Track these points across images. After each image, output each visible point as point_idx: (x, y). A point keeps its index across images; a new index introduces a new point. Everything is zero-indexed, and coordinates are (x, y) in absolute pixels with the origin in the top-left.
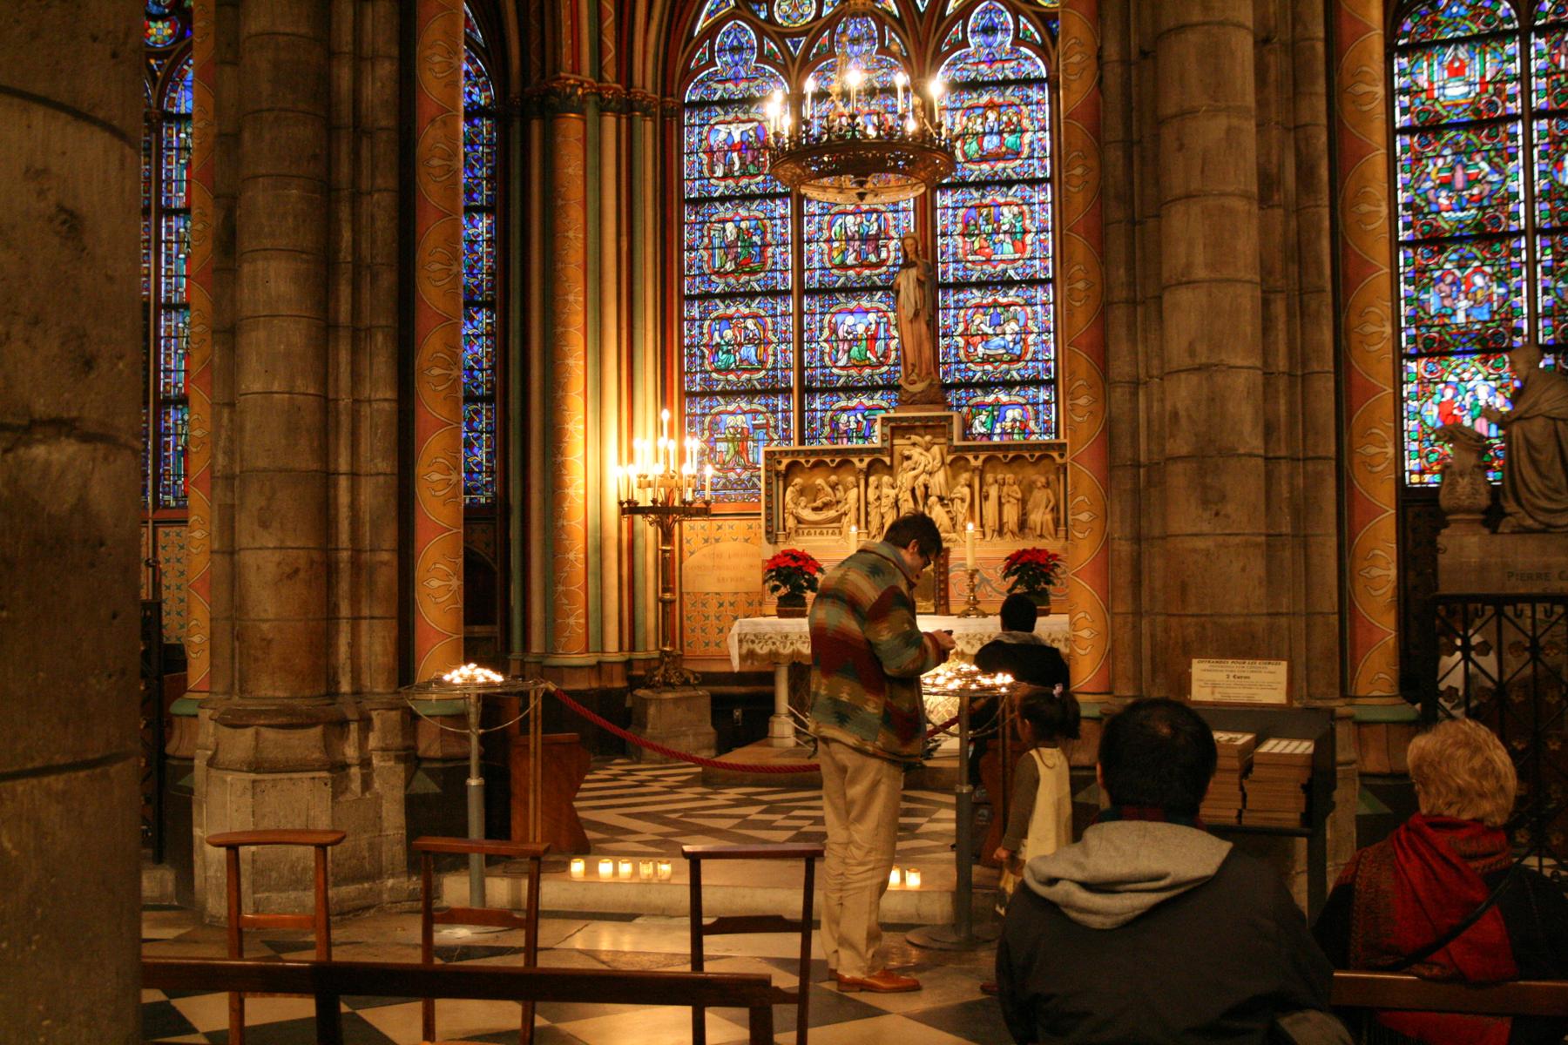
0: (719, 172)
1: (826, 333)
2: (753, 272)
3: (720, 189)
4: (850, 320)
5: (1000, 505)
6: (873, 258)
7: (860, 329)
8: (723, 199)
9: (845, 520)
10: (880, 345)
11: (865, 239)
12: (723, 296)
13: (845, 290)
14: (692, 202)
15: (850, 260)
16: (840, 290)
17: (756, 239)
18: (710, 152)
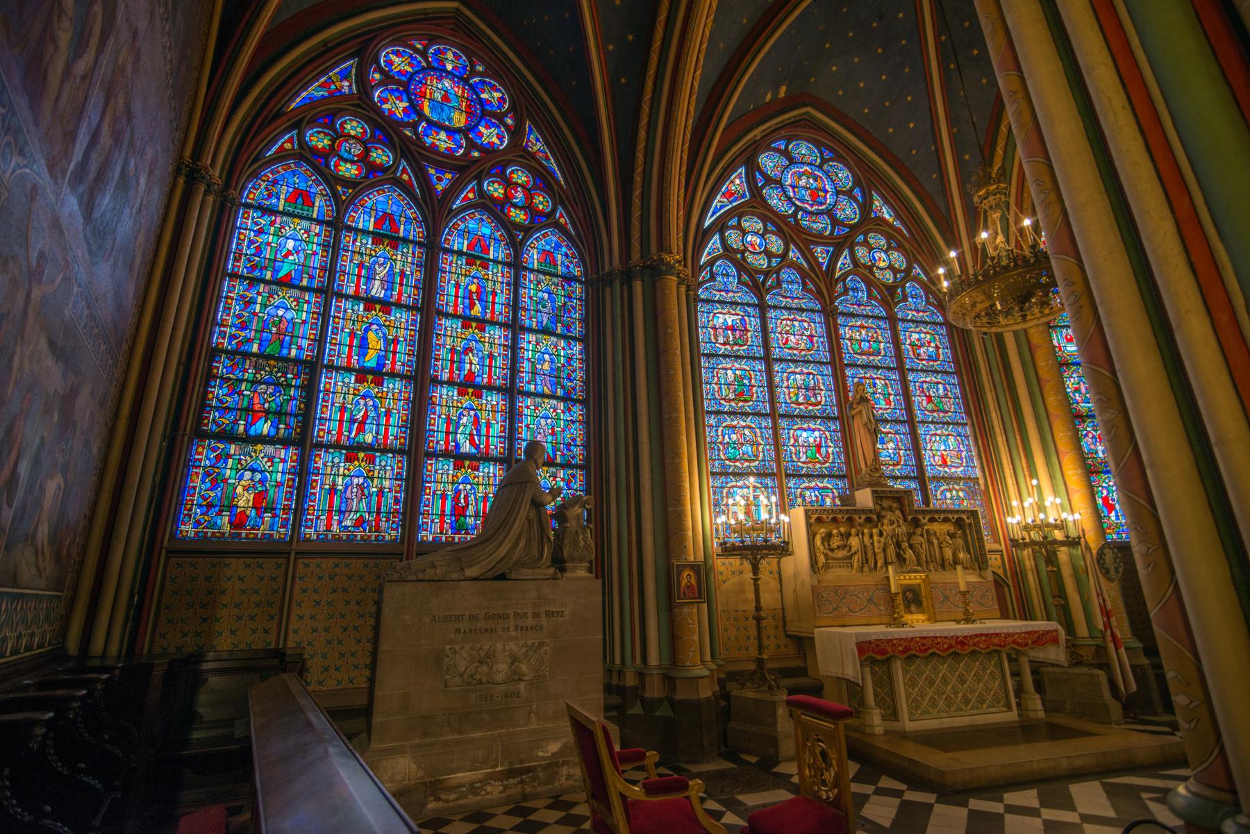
0: (721, 340)
1: (792, 441)
2: (746, 401)
3: (723, 350)
4: (805, 434)
5: (941, 548)
6: (813, 400)
7: (811, 440)
8: (725, 356)
9: (856, 558)
10: (823, 450)
11: (807, 389)
12: (729, 413)
13: (802, 417)
14: (704, 355)
15: (801, 400)
16: (797, 416)
17: (746, 381)
18: (714, 328)
